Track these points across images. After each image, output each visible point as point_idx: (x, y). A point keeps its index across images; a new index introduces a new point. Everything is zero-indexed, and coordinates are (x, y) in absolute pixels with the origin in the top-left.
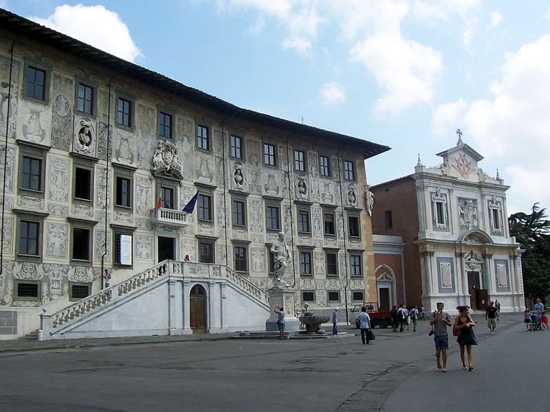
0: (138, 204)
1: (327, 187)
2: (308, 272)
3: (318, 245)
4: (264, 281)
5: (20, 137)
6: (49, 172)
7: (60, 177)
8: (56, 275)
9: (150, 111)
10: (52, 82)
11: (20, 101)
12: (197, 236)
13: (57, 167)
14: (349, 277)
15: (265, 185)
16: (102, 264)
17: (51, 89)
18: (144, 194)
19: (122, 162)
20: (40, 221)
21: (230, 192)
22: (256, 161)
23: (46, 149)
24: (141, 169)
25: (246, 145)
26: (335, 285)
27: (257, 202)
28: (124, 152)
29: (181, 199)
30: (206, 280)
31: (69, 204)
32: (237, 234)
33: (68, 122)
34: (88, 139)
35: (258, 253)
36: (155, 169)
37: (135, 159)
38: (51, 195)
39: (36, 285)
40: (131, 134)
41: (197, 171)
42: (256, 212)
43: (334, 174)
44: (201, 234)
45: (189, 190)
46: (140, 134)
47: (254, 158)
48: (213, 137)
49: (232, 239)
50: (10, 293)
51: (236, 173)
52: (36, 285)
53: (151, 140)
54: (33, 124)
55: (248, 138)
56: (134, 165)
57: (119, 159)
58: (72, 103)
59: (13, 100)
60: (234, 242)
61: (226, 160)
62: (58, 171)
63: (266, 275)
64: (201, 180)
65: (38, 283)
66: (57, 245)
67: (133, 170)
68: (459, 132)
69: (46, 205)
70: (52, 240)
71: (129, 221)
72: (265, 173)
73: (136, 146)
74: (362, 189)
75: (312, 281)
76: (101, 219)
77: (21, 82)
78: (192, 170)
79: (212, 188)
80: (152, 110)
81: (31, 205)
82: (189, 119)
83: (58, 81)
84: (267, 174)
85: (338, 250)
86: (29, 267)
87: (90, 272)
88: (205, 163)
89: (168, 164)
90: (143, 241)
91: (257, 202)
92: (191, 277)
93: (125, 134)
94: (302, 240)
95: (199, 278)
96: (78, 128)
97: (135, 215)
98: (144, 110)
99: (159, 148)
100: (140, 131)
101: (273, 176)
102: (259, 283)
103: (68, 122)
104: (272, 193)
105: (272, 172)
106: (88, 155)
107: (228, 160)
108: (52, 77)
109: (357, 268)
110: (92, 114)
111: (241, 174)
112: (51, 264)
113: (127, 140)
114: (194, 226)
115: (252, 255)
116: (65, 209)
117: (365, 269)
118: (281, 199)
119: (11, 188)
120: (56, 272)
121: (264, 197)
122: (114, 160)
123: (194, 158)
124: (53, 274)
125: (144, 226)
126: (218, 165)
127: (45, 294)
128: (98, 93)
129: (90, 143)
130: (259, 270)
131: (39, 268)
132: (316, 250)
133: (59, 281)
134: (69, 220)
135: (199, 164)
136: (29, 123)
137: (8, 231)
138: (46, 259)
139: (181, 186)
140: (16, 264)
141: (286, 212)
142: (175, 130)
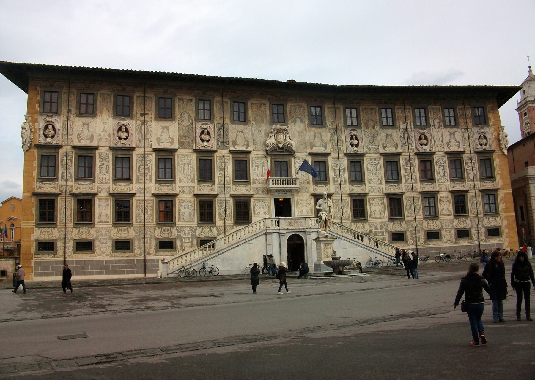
0: (255, 177)
1: (452, 136)
2: (432, 213)
3: (443, 188)
4: (384, 225)
5: (156, 146)
7: (186, 167)
8: (187, 234)
9: (263, 106)
10: (176, 105)
11: (154, 122)
14: (481, 215)
15: (383, 144)
16: (225, 223)
17: (176, 109)
18: (260, 169)
19: (238, 148)
20: (173, 199)
21: (346, 155)
22: (372, 125)
23: (175, 150)
24: (257, 151)
25: (361, 113)
26: (463, 223)
27: (375, 159)
28: (240, 140)
30: (302, 230)
31: (195, 185)
32: (354, 188)
34: (207, 137)
35: (377, 202)
36: (268, 148)
37: (251, 143)
38: (180, 181)
39: (172, 241)
41: (311, 143)
42: (374, 169)
43: (461, 122)
44: (317, 192)
46: (254, 125)
47: (371, 123)
48: (326, 113)
49: (349, 192)
50: (154, 247)
51: (351, 138)
52: (172, 241)
53: (265, 127)
54: (164, 136)
55: (364, 107)
56: (249, 149)
57: (236, 147)
58: (193, 115)
59: (149, 123)
60: (350, 195)
61: (341, 129)
62: (185, 164)
63: (386, 219)
64: (315, 150)
65: (174, 240)
66: (187, 214)
67: (249, 152)
68: (530, 67)
70: (183, 210)
71: (248, 190)
72: (382, 134)
73: (253, 135)
74: (495, 130)
75: (438, 222)
76: (222, 192)
77: (154, 110)
78: (306, 144)
79: (327, 155)
80: (264, 104)
81: (166, 189)
82: (300, 104)
83: (181, 102)
84: (384, 134)
85: (467, 191)
86: (166, 230)
87: (214, 230)
88: (318, 135)
89: (280, 143)
90: (262, 203)
91: (375, 159)
92: (288, 229)
93: (240, 127)
94: (426, 186)
95: (296, 229)
96: (199, 131)
97: (252, 185)
98: (257, 106)
99: (271, 132)
100: (254, 122)
101: (391, 135)
102: (379, 227)
103: (190, 129)
104: (391, 150)
105: (390, 131)
106: (208, 148)
107: (343, 130)
108: (176, 100)
109: (493, 206)
110: (210, 119)
111: (356, 139)
112: (182, 227)
113: (242, 132)
115: (371, 204)
117: (502, 206)
118: (399, 154)
119: (151, 180)
120: (187, 232)
121: (382, 155)
122: (232, 148)
123: (307, 133)
124: (184, 233)
125: (260, 192)
126: (332, 135)
127: (179, 247)
128: (215, 103)
129: (209, 140)
130: (378, 216)
131: (174, 230)
132: (441, 194)
133: (189, 238)
134: (196, 196)
135: (313, 137)
136: (161, 135)
137: (150, 208)
138: (178, 224)
139: (294, 158)
140: (157, 228)
141: (407, 164)
142: (287, 116)
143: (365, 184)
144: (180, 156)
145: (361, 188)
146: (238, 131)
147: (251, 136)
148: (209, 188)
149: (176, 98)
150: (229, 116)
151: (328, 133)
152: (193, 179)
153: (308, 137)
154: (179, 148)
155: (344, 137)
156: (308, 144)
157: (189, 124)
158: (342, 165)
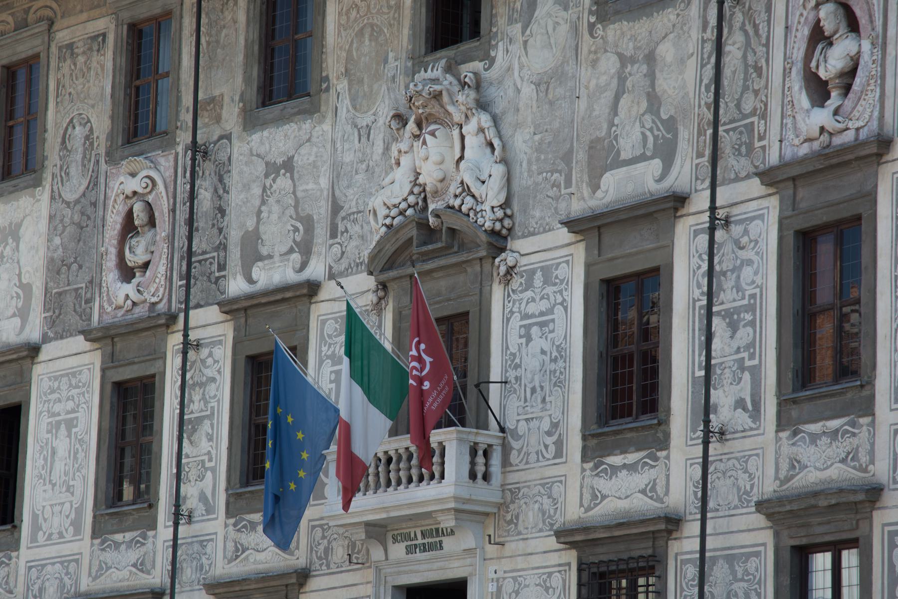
6: (36, 440)
12: (568, 536)
13: (57, 408)
23: (33, 350)
29: (505, 347)
31: (84, 545)
33: (91, 204)
37: (321, 232)
38: (36, 528)
40: (307, 125)
41: (593, 146)
45: (547, 281)
46: (345, 105)
56: (316, 270)
57: (256, 273)
67: (312, 289)
69: (22, 571)
78: (567, 158)
83: (66, 66)
93: (278, 139)
96: (114, 220)
100: (342, 86)
114: (562, 480)
116: (72, 567)
122: (236, 286)
123: (585, 73)
135: (609, 95)
143: (868, 408)
144: (46, 384)
145: (841, 447)
146: (272, 170)
147: (324, 182)
148: (133, 555)
149: (54, 49)
150: (239, 79)
151: (695, 34)
152: (79, 511)
153: (583, 104)
154: (46, 339)
155: (778, 31)
156: (580, 156)
157: (85, 183)
158: (747, 273)
